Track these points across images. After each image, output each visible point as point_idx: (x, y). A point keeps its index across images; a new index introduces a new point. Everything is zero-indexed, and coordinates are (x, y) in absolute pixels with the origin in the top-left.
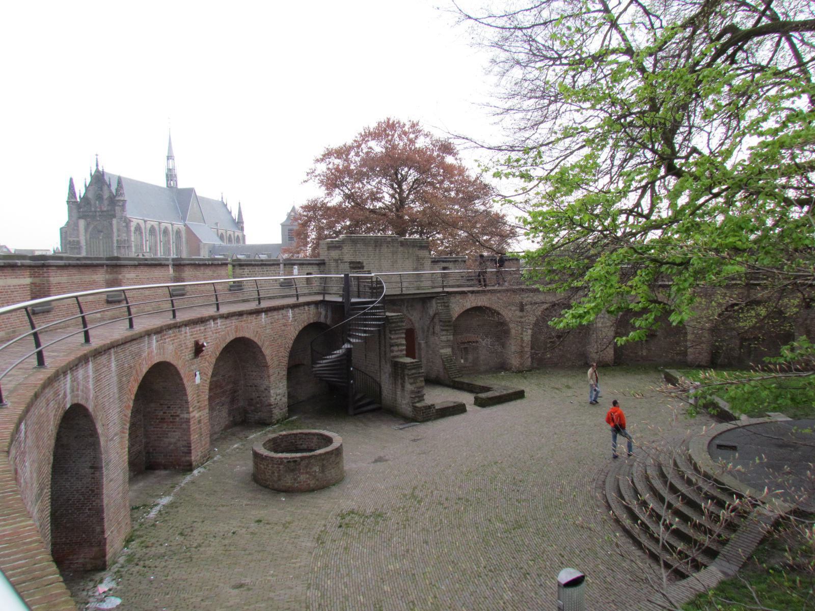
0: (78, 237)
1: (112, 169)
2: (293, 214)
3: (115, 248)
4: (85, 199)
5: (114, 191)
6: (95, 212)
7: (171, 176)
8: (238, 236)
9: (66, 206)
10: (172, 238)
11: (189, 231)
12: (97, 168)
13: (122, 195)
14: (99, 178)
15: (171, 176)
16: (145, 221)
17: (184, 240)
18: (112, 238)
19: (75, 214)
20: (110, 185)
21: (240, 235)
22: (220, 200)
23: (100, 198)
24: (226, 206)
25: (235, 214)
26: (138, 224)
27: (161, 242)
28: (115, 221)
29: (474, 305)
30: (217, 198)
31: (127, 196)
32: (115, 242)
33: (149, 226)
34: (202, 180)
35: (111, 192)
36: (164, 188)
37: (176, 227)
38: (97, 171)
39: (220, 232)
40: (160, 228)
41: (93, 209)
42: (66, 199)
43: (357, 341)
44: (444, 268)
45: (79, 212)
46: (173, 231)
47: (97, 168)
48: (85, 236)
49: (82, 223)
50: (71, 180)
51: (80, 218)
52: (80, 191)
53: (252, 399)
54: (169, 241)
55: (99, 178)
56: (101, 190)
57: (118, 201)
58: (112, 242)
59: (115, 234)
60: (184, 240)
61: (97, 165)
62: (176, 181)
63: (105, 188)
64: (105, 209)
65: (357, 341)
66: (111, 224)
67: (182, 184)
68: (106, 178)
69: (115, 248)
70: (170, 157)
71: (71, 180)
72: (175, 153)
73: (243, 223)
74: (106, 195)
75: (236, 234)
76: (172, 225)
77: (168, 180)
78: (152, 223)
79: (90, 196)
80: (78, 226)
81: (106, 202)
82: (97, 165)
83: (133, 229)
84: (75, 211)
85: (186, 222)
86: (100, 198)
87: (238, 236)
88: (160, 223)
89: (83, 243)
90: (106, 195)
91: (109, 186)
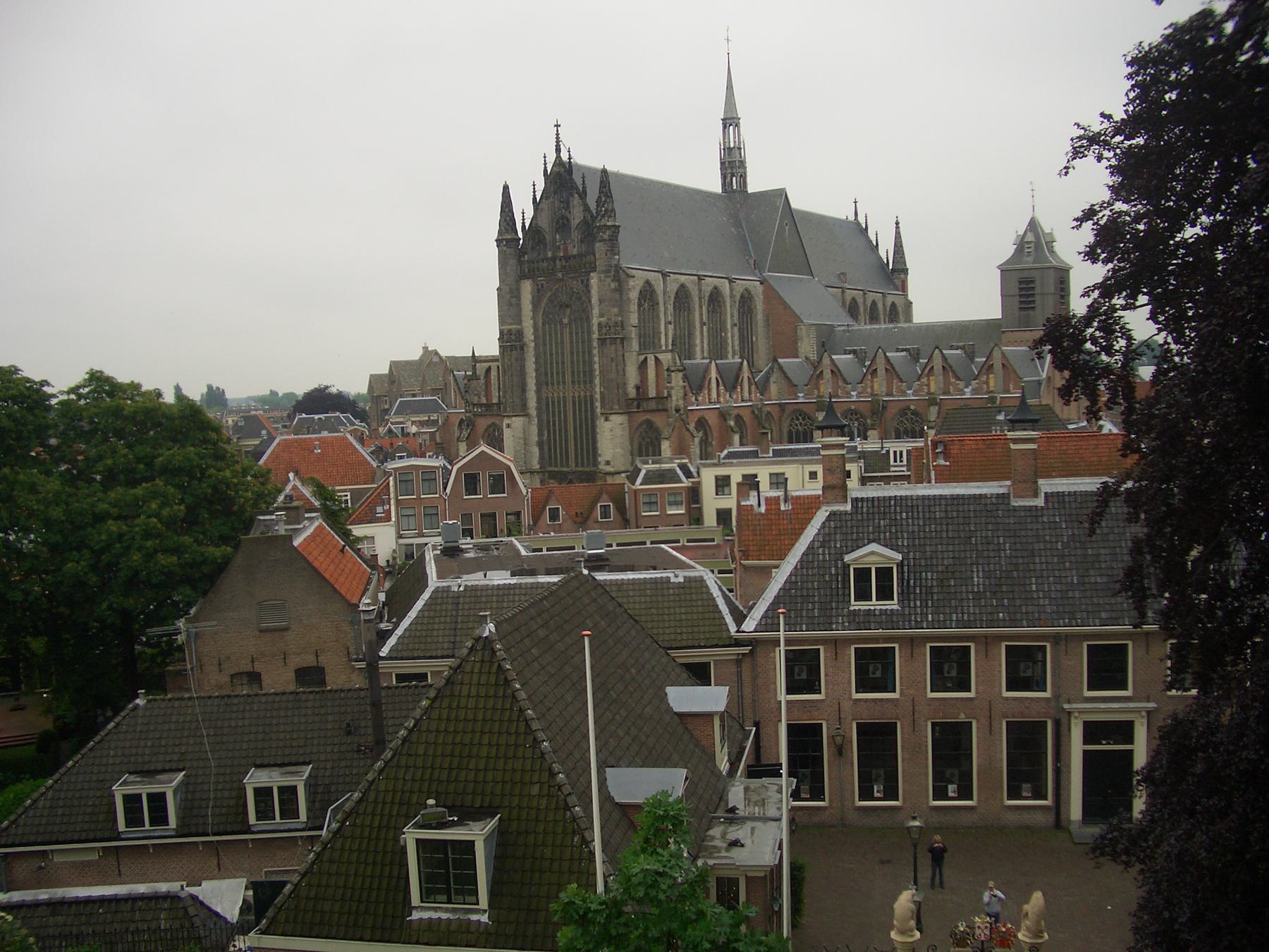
0: (520, 322)
1: (589, 155)
2: (1030, 237)
3: (595, 344)
4: (533, 231)
5: (593, 206)
6: (554, 259)
7: (732, 165)
8: (893, 304)
10: (731, 314)
11: (771, 294)
12: (558, 157)
13: (611, 213)
14: (562, 179)
15: (732, 165)
16: (665, 275)
17: (760, 317)
18: (588, 320)
20: (585, 191)
21: (899, 302)
22: (852, 218)
23: (562, 225)
25: (886, 249)
26: (648, 282)
27: (703, 324)
28: (594, 281)
30: (842, 212)
31: (623, 217)
32: (595, 328)
33: (673, 288)
34: (806, 171)
35: (586, 208)
36: (716, 194)
37: (739, 287)
39: (849, 294)
40: (700, 290)
41: (550, 254)
42: (495, 236)
45: (520, 263)
46: (732, 296)
47: (558, 157)
48: (534, 318)
49: (527, 288)
50: (506, 188)
51: (523, 277)
52: (524, 209)
54: (723, 323)
56: (567, 207)
57: (599, 228)
58: (590, 332)
59: (596, 311)
60: (760, 317)
61: (558, 150)
62: (743, 177)
63: (576, 200)
64: (575, 252)
66: (587, 287)
67: (756, 183)
68: (577, 178)
69: (595, 344)
70: (730, 121)
71: (506, 188)
73: (905, 271)
74: (577, 216)
75: (890, 300)
76: (731, 281)
77: (724, 177)
78: (683, 278)
79: (544, 223)
80: (519, 298)
81: (576, 235)
82: (558, 150)
83: (634, 295)
84: (513, 262)
85: (766, 274)
86: (562, 225)
87: (893, 304)
88: (700, 278)
89: (529, 335)
90: (577, 216)
91: (583, 195)
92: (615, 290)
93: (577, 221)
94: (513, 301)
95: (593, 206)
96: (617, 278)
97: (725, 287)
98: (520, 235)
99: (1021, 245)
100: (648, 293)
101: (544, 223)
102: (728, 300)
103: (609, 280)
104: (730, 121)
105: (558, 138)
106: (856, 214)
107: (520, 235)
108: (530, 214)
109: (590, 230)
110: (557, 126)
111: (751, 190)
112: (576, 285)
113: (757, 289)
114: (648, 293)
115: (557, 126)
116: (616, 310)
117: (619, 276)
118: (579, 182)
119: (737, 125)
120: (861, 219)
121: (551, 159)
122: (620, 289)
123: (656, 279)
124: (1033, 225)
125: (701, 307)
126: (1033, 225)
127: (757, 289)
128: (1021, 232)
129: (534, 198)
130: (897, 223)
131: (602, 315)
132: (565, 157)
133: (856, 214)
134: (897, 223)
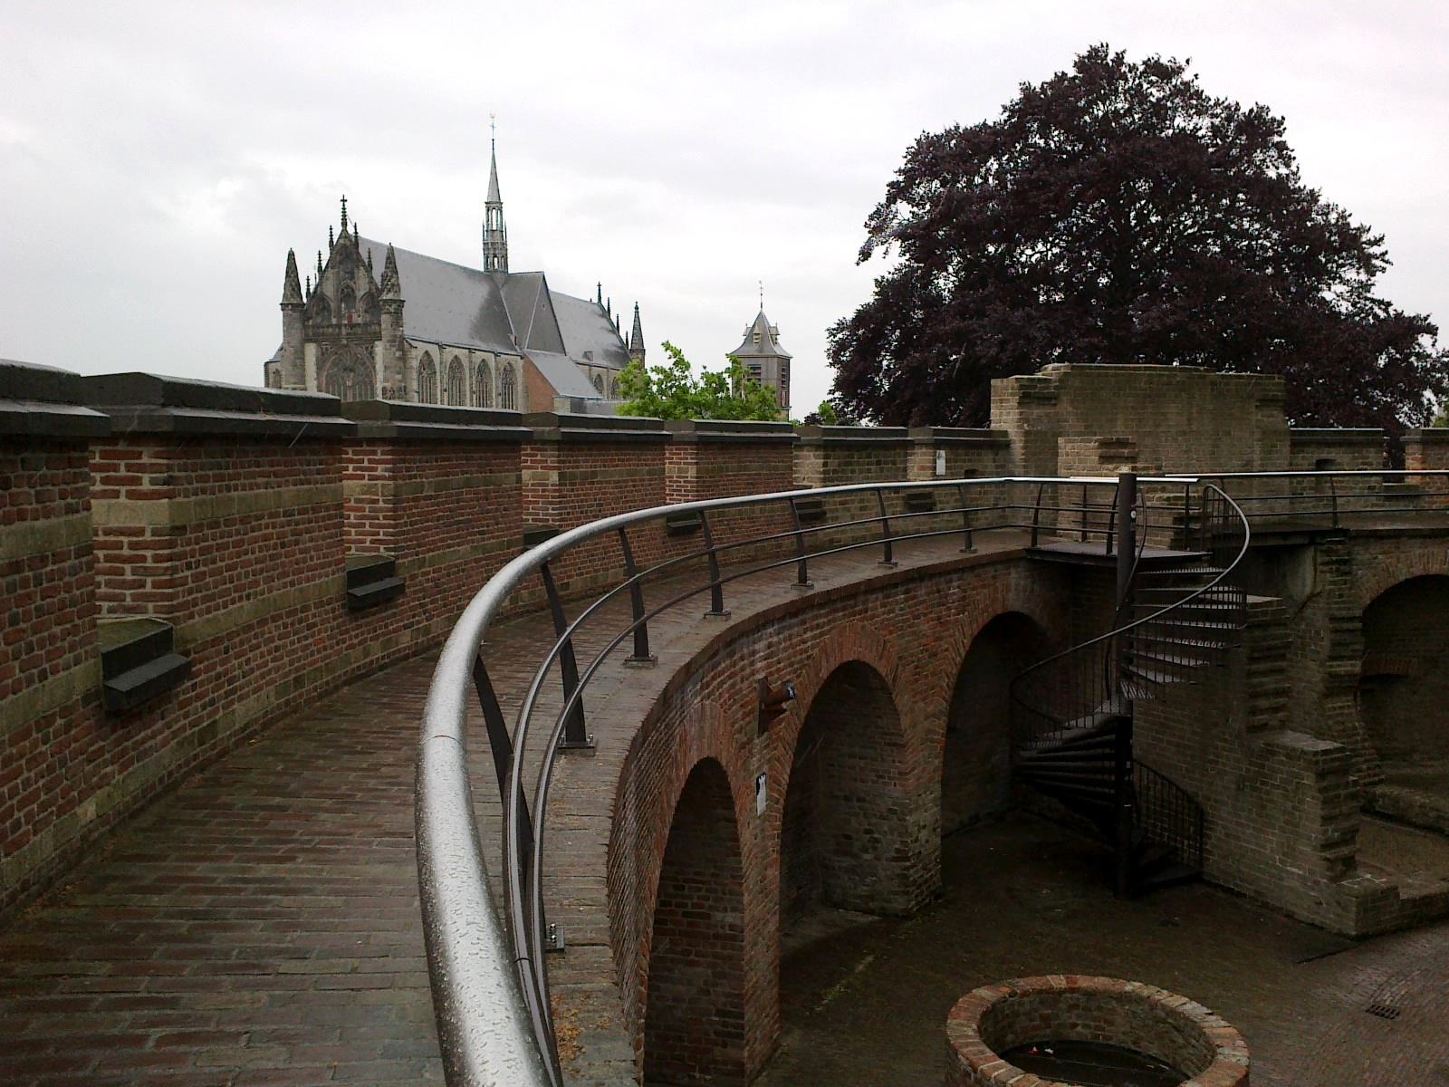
1: (375, 229)
4: (317, 296)
5: (378, 279)
6: (339, 326)
7: (495, 244)
11: (530, 368)
13: (396, 287)
14: (347, 251)
15: (495, 244)
19: (297, 335)
20: (370, 265)
22: (595, 300)
23: (347, 295)
25: (626, 329)
26: (427, 352)
27: (472, 392)
28: (379, 348)
29: (1418, 570)
31: (409, 288)
36: (479, 272)
39: (596, 371)
41: (334, 321)
43: (1168, 679)
44: (1321, 464)
45: (305, 327)
46: (497, 369)
48: (318, 379)
49: (311, 350)
50: (291, 255)
51: (309, 340)
52: (308, 272)
53: (848, 837)
55: (347, 251)
56: (352, 278)
59: (380, 376)
61: (344, 224)
62: (505, 257)
64: (360, 320)
65: (1168, 679)
68: (363, 252)
70: (494, 205)
71: (291, 255)
74: (362, 287)
77: (487, 258)
78: (457, 352)
79: (329, 290)
80: (303, 359)
81: (360, 306)
82: (344, 224)
83: (415, 363)
84: (298, 325)
86: (347, 295)
90: (362, 287)
92: (399, 358)
93: (362, 293)
94: (298, 361)
95: (378, 279)
96: (401, 348)
97: (491, 358)
99: (751, 336)
100: (427, 361)
101: (329, 290)
102: (493, 372)
103: (394, 349)
104: (494, 205)
105: (344, 209)
107: (305, 300)
108: (313, 283)
109: (374, 302)
110: (344, 201)
111: (513, 268)
112: (361, 351)
113: (519, 364)
114: (427, 361)
115: (344, 201)
116: (399, 377)
117: (402, 345)
118: (364, 256)
119: (500, 209)
120: (605, 303)
121: (337, 231)
122: (404, 358)
123: (434, 350)
124: (761, 317)
125: (471, 377)
126: (761, 317)
127: (519, 364)
129: (320, 267)
130: (637, 308)
131: (386, 380)
132: (351, 230)
134: (637, 308)
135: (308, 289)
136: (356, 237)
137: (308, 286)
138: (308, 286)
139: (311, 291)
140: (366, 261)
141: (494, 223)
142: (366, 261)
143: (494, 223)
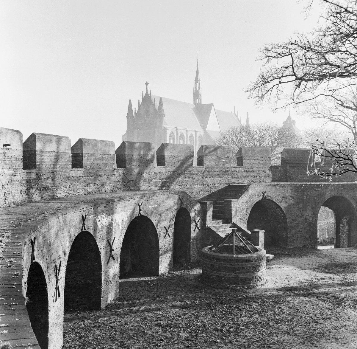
1: (155, 93)
4: (138, 114)
7: (197, 94)
9: (126, 120)
14: (147, 99)
15: (197, 94)
20: (154, 103)
22: (233, 112)
24: (237, 117)
38: (147, 93)
50: (130, 101)
52: (135, 107)
62: (201, 99)
70: (197, 81)
71: (130, 101)
72: (201, 78)
82: (147, 90)
98: (134, 115)
104: (197, 81)
106: (235, 111)
107: (134, 115)
108: (137, 109)
118: (153, 100)
120: (236, 113)
126: (289, 118)
128: (285, 120)
130: (248, 114)
132: (149, 92)
133: (235, 111)
134: (248, 114)
135: (135, 113)
136: (150, 93)
137: (135, 111)
138: (135, 111)
139: (136, 112)
140: (153, 103)
141: (197, 87)
142: (153, 103)
143: (197, 87)
